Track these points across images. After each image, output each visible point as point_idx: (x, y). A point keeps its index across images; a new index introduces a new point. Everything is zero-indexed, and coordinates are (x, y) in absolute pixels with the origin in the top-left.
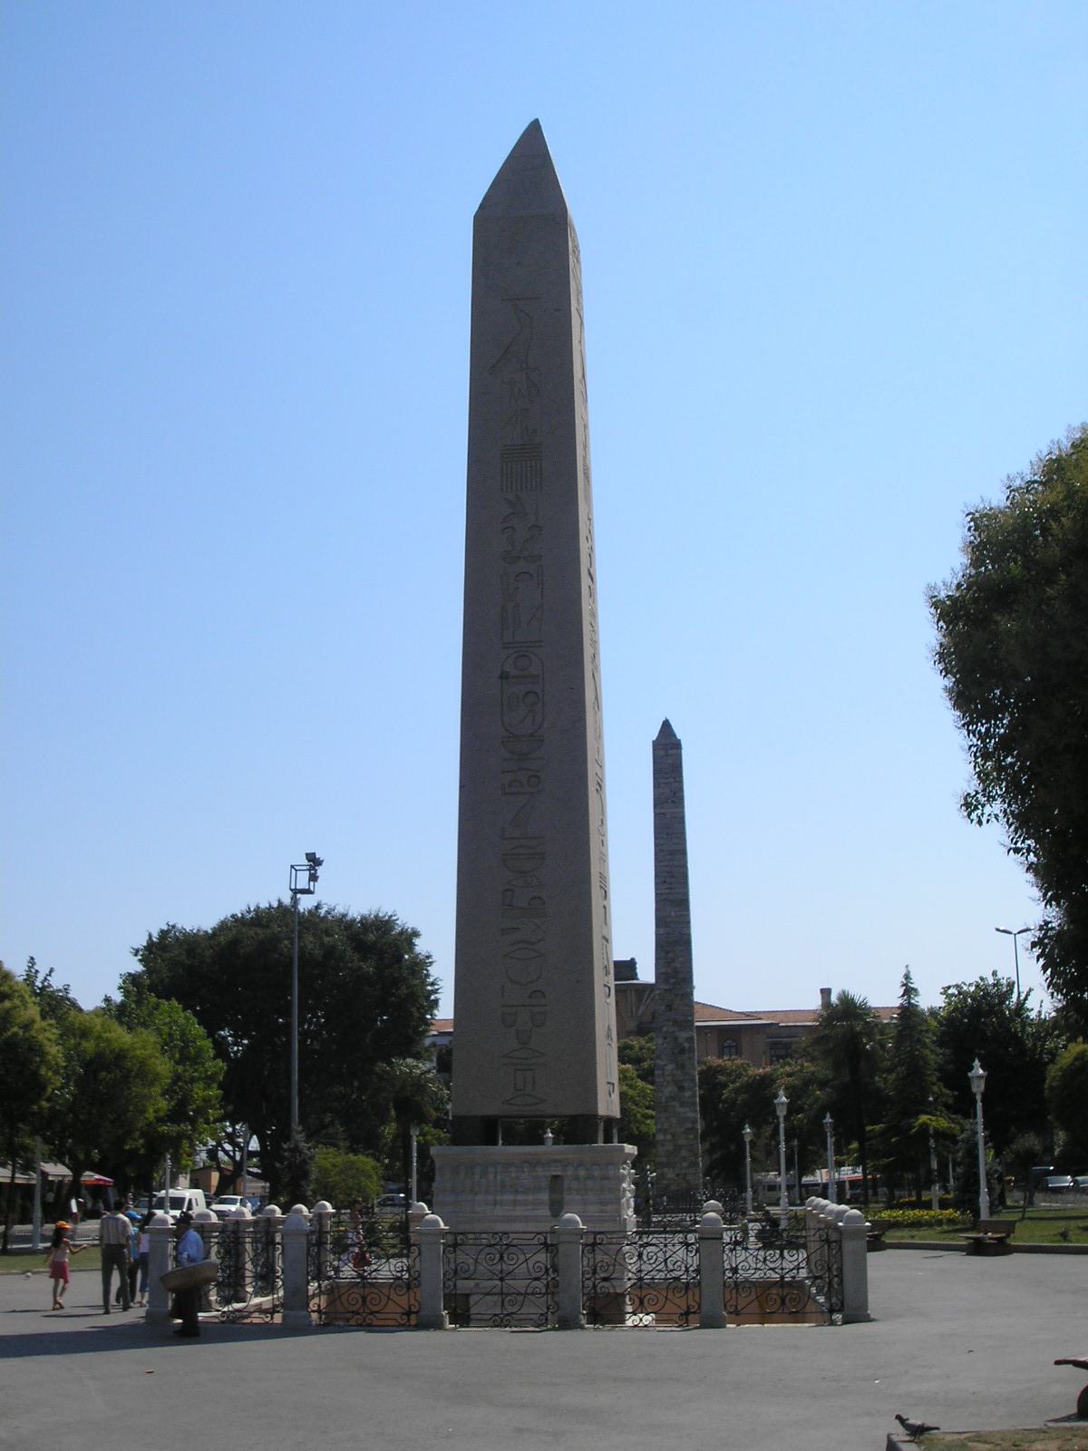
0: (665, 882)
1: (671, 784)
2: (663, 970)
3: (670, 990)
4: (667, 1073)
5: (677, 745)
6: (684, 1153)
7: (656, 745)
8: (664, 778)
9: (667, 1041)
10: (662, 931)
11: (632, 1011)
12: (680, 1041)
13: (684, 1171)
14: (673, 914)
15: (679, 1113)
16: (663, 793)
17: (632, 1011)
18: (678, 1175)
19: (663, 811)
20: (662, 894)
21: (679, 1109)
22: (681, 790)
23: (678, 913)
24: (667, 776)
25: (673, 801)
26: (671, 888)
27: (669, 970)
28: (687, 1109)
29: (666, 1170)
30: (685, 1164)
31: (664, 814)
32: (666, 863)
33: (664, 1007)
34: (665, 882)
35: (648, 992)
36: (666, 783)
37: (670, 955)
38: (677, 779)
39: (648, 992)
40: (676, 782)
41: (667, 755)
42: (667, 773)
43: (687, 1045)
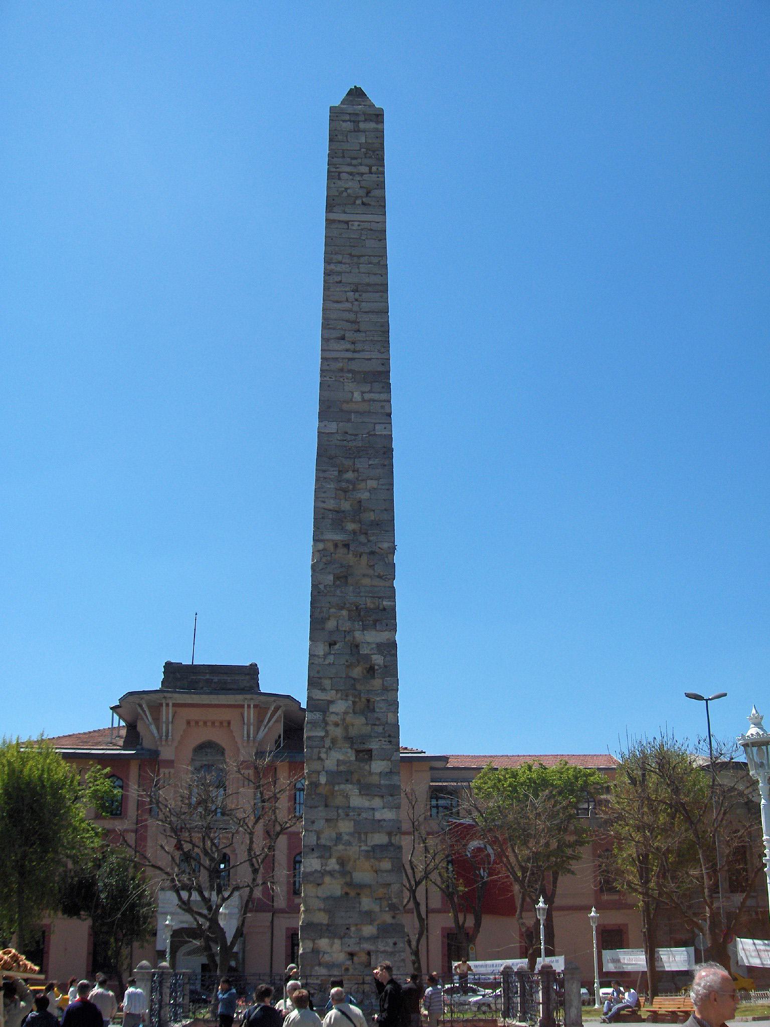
0: (343, 338)
1: (362, 174)
2: (331, 504)
3: (347, 546)
4: (332, 718)
5: (378, 116)
6: (367, 903)
7: (335, 114)
8: (350, 165)
9: (337, 647)
10: (333, 427)
11: (248, 736)
12: (364, 651)
13: (367, 946)
14: (357, 396)
15: (359, 810)
16: (346, 189)
17: (248, 736)
18: (352, 955)
19: (343, 217)
20: (336, 359)
21: (357, 801)
22: (381, 185)
23: (367, 396)
24: (354, 162)
25: (363, 204)
26: (355, 351)
27: (346, 506)
28: (377, 802)
29: (323, 943)
30: (369, 930)
31: (347, 223)
32: (347, 305)
33: (331, 577)
34: (343, 338)
36: (351, 174)
37: (350, 475)
38: (374, 169)
40: (371, 173)
41: (359, 131)
42: (356, 159)
43: (378, 659)
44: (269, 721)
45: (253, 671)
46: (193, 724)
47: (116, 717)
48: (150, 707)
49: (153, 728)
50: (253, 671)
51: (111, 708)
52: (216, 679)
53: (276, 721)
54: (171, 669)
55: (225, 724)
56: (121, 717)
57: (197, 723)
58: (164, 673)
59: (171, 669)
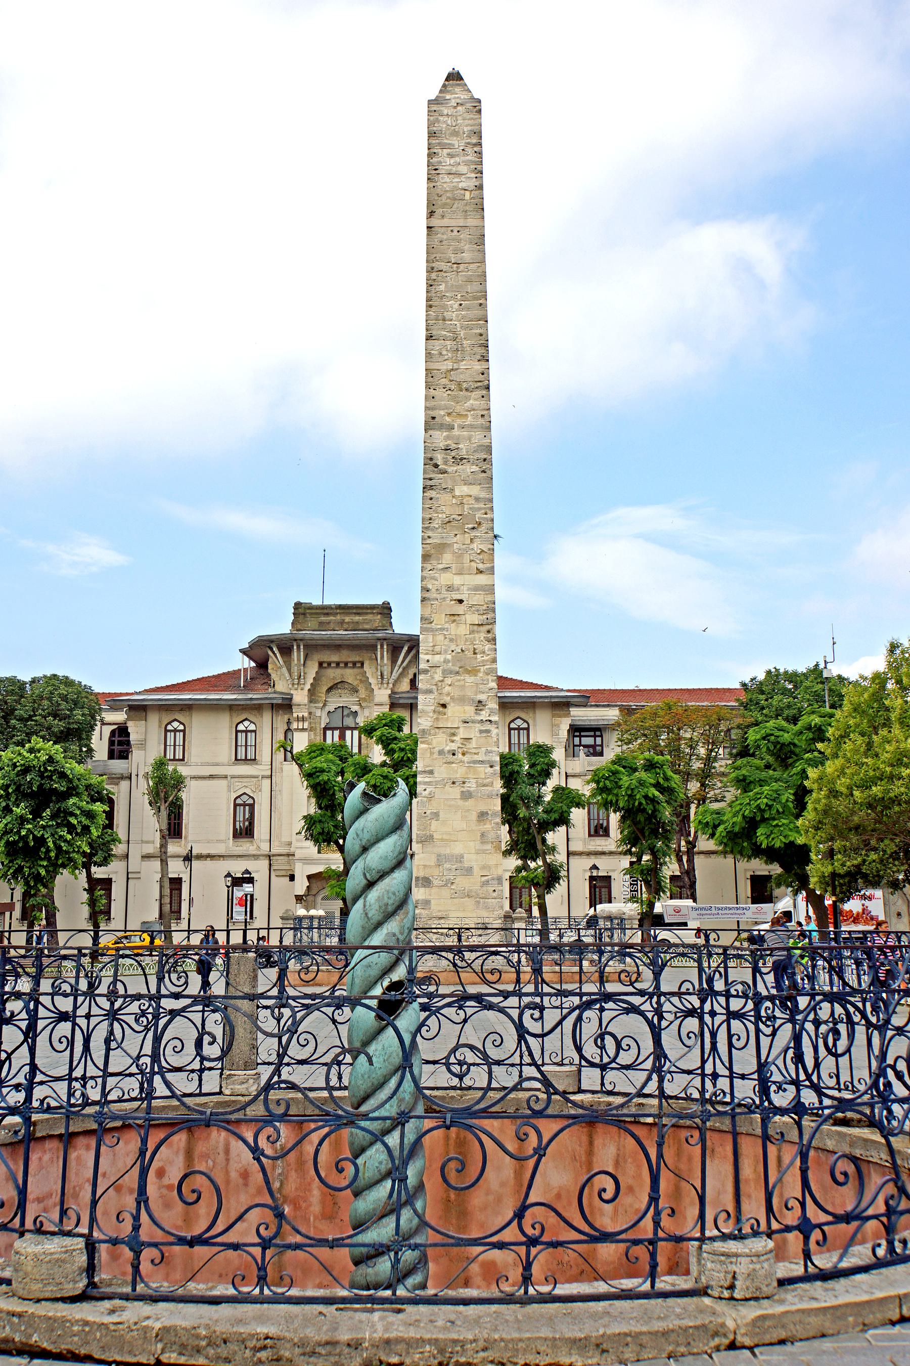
35: (406, 648)
39: (406, 648)
44: (403, 662)
45: (385, 610)
46: (325, 665)
47: (246, 659)
48: (279, 649)
49: (284, 670)
50: (385, 610)
51: (241, 651)
52: (347, 619)
53: (410, 662)
54: (300, 610)
55: (359, 665)
56: (251, 658)
57: (329, 664)
58: (294, 614)
59: (300, 610)
